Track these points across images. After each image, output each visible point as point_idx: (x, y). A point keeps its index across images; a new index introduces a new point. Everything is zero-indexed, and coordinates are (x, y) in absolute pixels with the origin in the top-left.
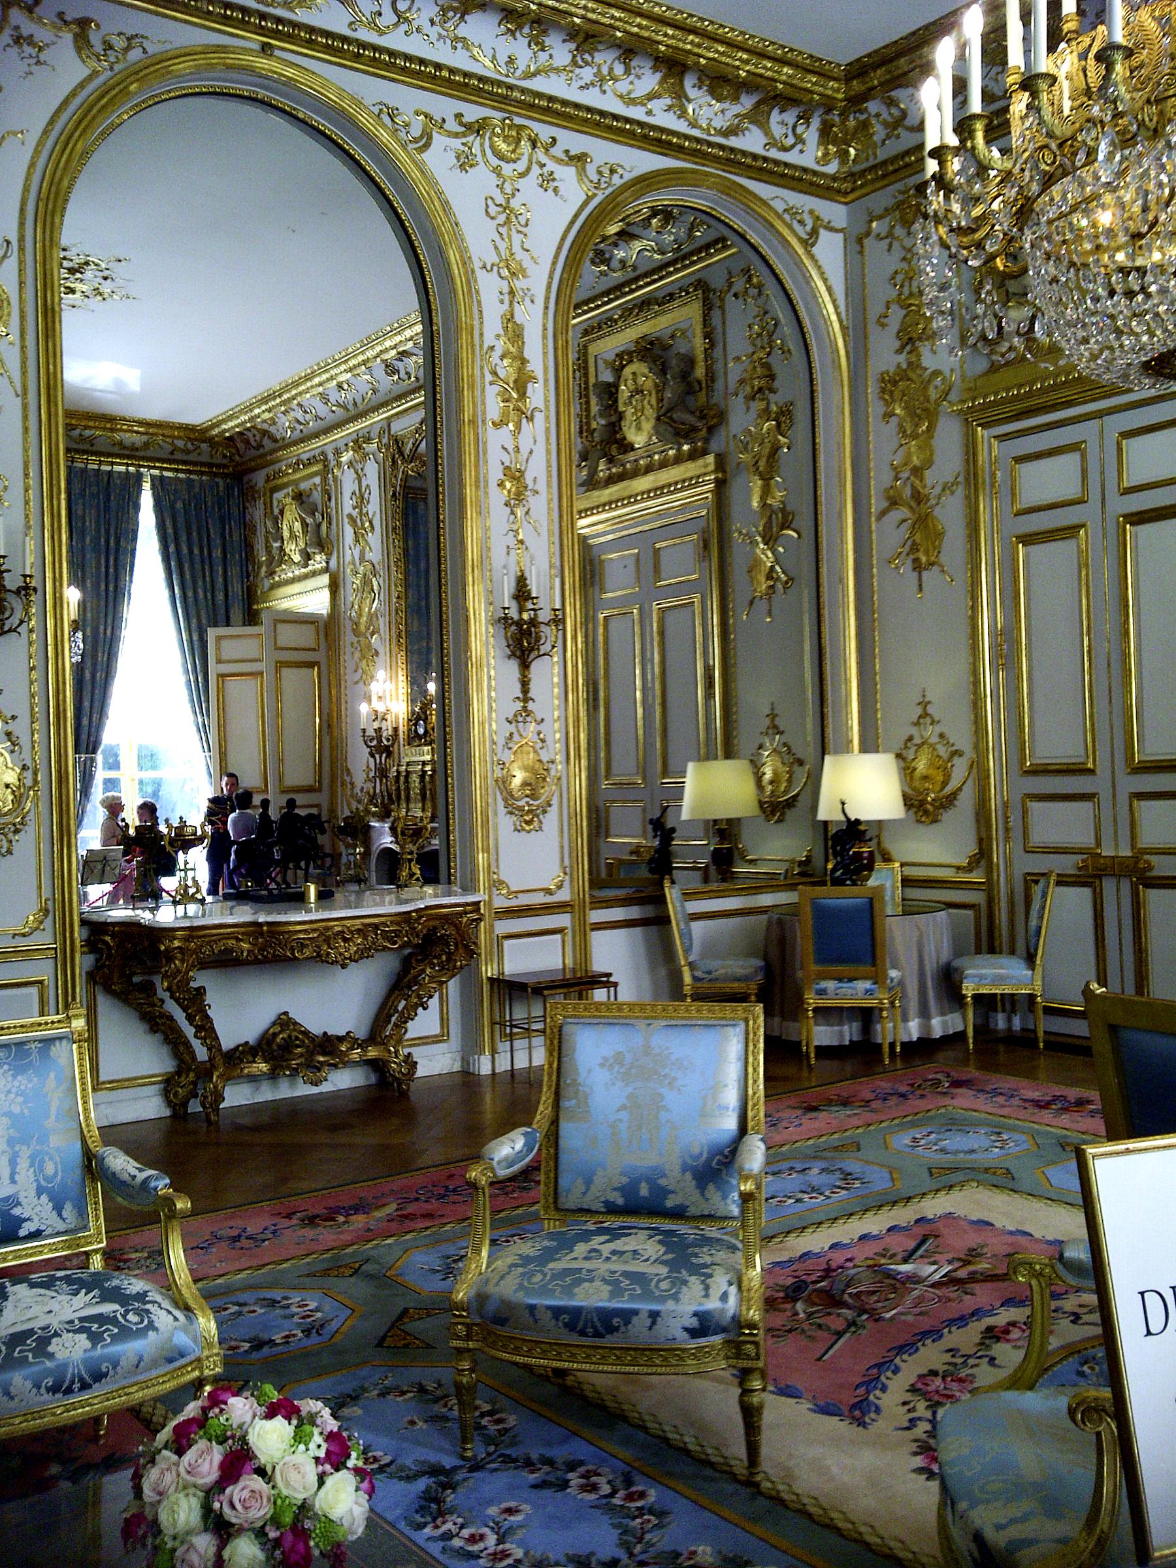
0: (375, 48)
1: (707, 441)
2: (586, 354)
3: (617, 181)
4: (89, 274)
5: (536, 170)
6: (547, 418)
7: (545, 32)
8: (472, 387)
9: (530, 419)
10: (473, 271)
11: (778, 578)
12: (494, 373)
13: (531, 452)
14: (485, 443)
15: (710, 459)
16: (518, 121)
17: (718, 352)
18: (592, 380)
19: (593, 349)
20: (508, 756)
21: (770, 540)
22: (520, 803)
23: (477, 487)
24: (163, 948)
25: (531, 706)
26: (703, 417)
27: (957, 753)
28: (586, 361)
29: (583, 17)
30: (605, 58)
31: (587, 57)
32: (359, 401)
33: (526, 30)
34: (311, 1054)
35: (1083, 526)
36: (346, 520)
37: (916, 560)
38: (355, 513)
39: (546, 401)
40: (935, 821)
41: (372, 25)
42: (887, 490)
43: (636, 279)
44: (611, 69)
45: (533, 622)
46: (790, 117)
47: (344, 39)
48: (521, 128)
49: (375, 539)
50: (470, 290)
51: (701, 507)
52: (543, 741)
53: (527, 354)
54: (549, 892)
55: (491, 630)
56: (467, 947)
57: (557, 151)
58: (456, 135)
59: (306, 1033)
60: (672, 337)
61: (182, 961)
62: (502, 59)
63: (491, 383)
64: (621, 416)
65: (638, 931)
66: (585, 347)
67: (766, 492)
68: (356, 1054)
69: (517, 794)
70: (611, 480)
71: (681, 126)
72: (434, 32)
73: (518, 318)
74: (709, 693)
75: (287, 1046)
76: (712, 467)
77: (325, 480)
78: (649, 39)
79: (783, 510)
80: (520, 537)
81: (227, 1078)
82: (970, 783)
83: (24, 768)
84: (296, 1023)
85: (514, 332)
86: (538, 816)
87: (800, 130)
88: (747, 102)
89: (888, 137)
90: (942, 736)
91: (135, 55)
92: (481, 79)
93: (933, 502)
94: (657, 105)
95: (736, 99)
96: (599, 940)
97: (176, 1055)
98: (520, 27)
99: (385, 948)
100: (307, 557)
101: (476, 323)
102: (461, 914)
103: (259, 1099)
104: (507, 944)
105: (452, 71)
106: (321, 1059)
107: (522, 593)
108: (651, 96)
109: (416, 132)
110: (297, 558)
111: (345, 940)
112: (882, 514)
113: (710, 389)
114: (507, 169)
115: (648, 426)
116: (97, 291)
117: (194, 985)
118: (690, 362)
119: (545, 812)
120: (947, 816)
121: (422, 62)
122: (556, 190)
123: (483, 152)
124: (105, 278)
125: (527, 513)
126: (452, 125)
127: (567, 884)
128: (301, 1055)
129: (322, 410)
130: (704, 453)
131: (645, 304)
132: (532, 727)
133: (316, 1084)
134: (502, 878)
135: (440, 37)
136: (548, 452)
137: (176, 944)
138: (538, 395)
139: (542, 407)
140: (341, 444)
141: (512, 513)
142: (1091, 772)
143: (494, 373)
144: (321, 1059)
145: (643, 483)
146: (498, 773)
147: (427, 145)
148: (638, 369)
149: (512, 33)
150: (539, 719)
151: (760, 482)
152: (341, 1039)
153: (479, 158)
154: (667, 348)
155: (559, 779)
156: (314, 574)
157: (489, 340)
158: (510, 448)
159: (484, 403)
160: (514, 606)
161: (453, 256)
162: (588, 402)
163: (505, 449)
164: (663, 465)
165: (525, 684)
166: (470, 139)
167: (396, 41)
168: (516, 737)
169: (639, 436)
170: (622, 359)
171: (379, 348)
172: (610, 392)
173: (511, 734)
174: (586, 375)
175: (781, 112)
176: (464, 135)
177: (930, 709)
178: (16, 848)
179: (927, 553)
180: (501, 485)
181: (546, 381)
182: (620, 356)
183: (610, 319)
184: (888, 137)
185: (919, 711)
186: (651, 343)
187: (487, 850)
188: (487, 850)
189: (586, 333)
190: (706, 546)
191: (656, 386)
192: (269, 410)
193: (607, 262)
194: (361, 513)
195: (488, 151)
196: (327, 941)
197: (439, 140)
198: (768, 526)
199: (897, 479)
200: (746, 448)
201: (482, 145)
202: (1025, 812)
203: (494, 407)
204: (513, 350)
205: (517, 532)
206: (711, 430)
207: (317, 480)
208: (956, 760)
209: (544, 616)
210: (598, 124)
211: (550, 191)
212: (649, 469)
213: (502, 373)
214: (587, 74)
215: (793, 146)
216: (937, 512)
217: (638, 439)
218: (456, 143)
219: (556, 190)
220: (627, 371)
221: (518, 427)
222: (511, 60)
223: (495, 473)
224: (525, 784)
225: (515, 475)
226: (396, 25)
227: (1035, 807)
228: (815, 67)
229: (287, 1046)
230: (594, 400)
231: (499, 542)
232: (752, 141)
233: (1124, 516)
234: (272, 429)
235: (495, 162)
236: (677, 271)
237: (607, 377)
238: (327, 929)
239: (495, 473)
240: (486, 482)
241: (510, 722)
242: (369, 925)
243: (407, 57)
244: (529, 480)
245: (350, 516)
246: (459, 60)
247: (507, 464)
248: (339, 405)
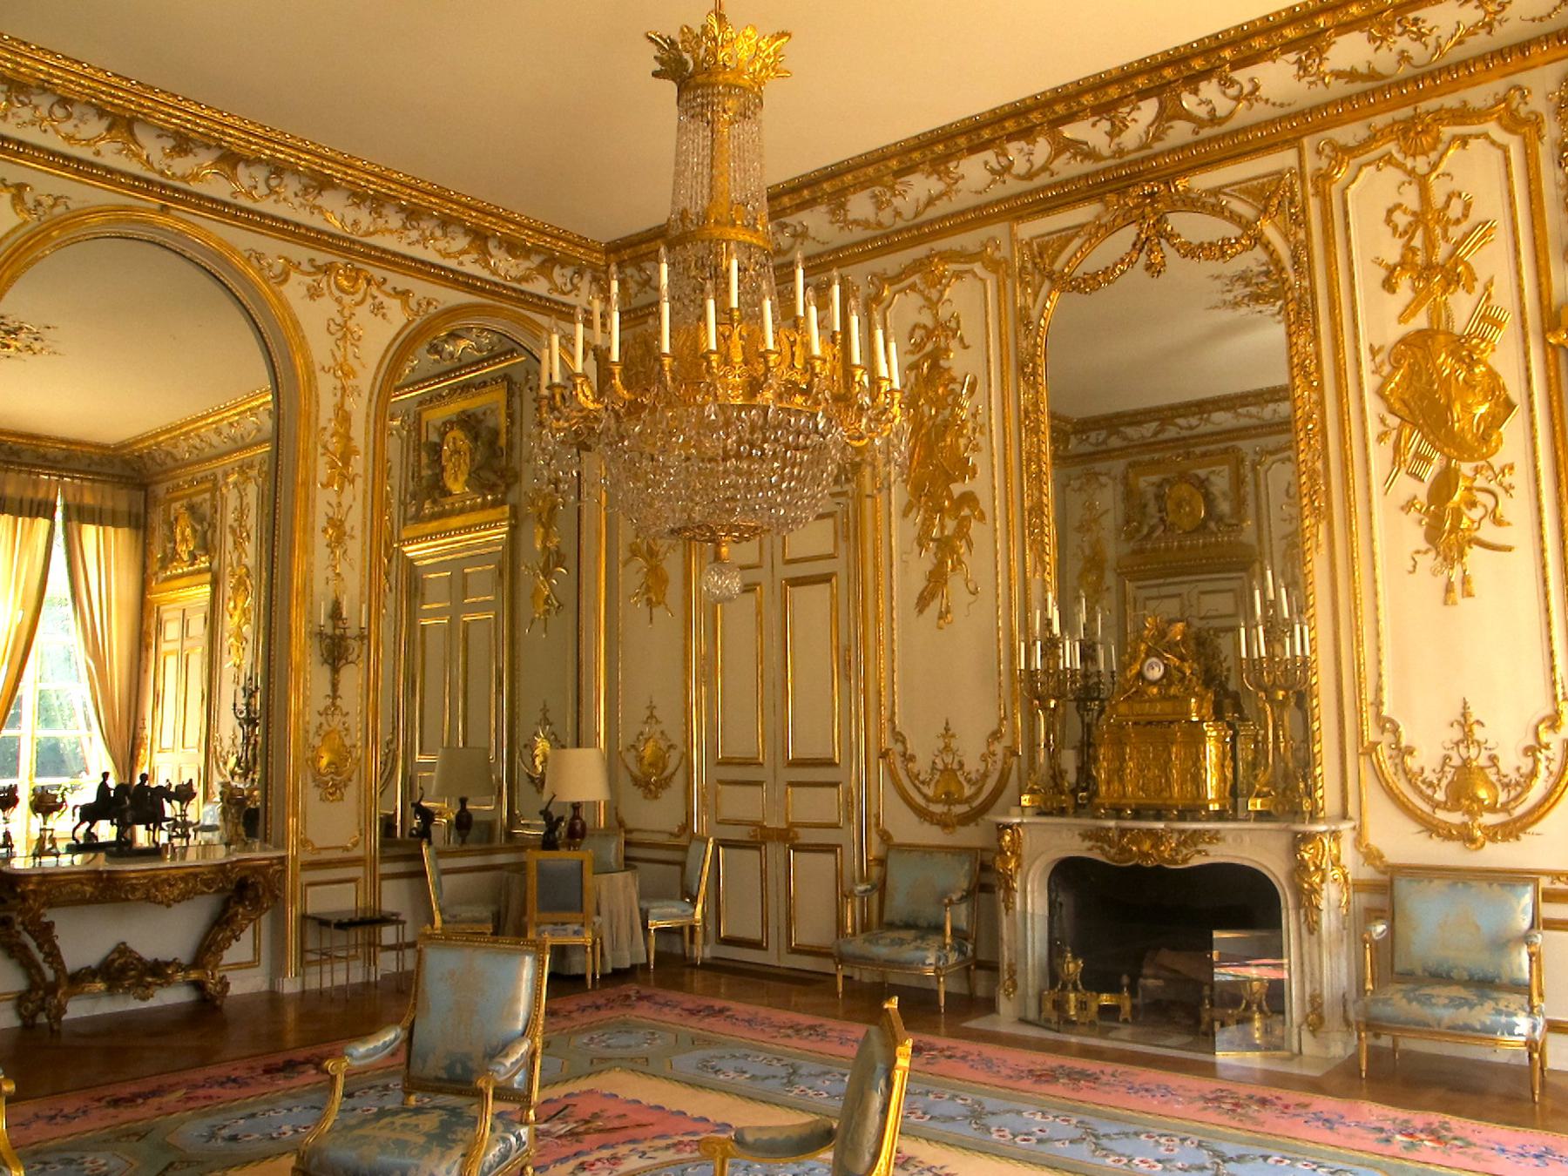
0: (249, 211)
1: (505, 494)
2: (420, 420)
3: (432, 310)
4: (22, 335)
5: (369, 300)
6: (365, 481)
7: (382, 206)
8: (306, 458)
9: (352, 482)
10: (314, 372)
11: (552, 605)
12: (325, 447)
14: (314, 500)
15: (507, 508)
16: (357, 265)
17: (516, 429)
18: (423, 439)
19: (426, 416)
20: (317, 741)
21: (547, 573)
22: (326, 779)
23: (305, 533)
24: (19, 890)
25: (338, 702)
26: (502, 477)
27: (671, 747)
28: (420, 425)
29: (407, 201)
30: (427, 225)
31: (415, 223)
32: (245, 435)
33: (368, 203)
34: (142, 975)
35: (759, 584)
36: (228, 530)
37: (649, 601)
38: (235, 525)
39: (366, 470)
40: (656, 797)
41: (249, 194)
42: (631, 545)
43: (460, 368)
44: (432, 234)
45: (343, 637)
46: (568, 272)
47: (226, 204)
48: (358, 270)
49: (250, 547)
50: (310, 385)
51: (497, 544)
52: (347, 729)
53: (352, 434)
54: (346, 849)
55: (309, 642)
56: (272, 892)
57: (387, 288)
58: (309, 274)
59: (140, 959)
60: (484, 414)
61: (35, 901)
62: (349, 221)
63: (323, 455)
64: (443, 469)
65: (404, 883)
66: (420, 414)
67: (546, 537)
68: (179, 976)
69: (322, 771)
70: (434, 517)
71: (485, 274)
72: (297, 201)
73: (347, 407)
74: (499, 691)
75: (123, 970)
76: (507, 515)
77: (213, 497)
78: (457, 218)
79: (558, 552)
81: (69, 995)
82: (681, 769)
84: (131, 951)
85: (344, 417)
87: (575, 281)
88: (536, 260)
89: (639, 291)
90: (662, 733)
91: (60, 209)
92: (331, 235)
93: (661, 557)
94: (466, 258)
95: (527, 257)
96: (388, 886)
97: (29, 976)
98: (363, 201)
99: (203, 893)
100: (194, 558)
101: (313, 410)
102: (268, 866)
103: (97, 1013)
104: (310, 890)
105: (308, 229)
106: (150, 979)
107: (336, 614)
108: (463, 252)
109: (277, 270)
110: (186, 557)
111: (170, 885)
112: (626, 563)
113: (509, 455)
114: (347, 299)
115: (463, 478)
116: (29, 347)
117: (45, 919)
118: (495, 433)
119: (345, 786)
120: (665, 795)
121: (285, 222)
122: (384, 316)
123: (329, 285)
124: (36, 339)
126: (306, 267)
127: (361, 844)
128: (132, 977)
129: (215, 440)
130: (503, 503)
131: (465, 387)
132: (337, 718)
133: (144, 999)
134: (308, 837)
135: (302, 205)
136: (364, 507)
137: (31, 887)
138: (358, 464)
139: (361, 472)
140: (229, 468)
142: (761, 764)
143: (325, 447)
144: (150, 979)
145: (456, 522)
146: (309, 754)
147: (285, 280)
148: (457, 433)
149: (358, 205)
150: (344, 711)
151: (542, 530)
152: (168, 964)
153: (326, 291)
154: (480, 422)
155: (359, 760)
156: (199, 572)
157: (322, 423)
159: (315, 470)
160: (330, 623)
161: (299, 361)
162: (419, 455)
163: (330, 504)
164: (473, 509)
165: (335, 686)
166: (319, 277)
167: (267, 206)
168: (325, 727)
169: (457, 486)
170: (449, 424)
171: (261, 401)
172: (436, 450)
173: (321, 724)
174: (419, 434)
175: (562, 268)
176: (314, 274)
177: (656, 713)
179: (656, 594)
180: (325, 531)
181: (366, 454)
182: (444, 424)
183: (440, 395)
184: (639, 291)
185: (648, 713)
186: (469, 416)
187: (295, 814)
188: (295, 814)
189: (421, 403)
190: (501, 574)
191: (470, 449)
192: (172, 438)
193: (439, 353)
194: (240, 526)
195: (333, 287)
196: (155, 886)
197: (294, 276)
198: (547, 563)
199: (637, 537)
200: (533, 504)
201: (328, 282)
202: (717, 794)
203: (323, 471)
204: (342, 431)
205: (335, 567)
206: (508, 487)
207: (207, 496)
208: (672, 752)
209: (353, 631)
210: (420, 271)
211: (380, 316)
212: (462, 511)
213: (331, 447)
214: (414, 235)
215: (571, 291)
216: (664, 565)
217: (457, 488)
218: (309, 280)
219: (384, 316)
220: (449, 437)
221: (341, 488)
222: (355, 223)
223: (321, 521)
224: (329, 765)
225: (336, 524)
226: (267, 196)
227: (726, 790)
228: (581, 242)
229: (123, 970)
230: (423, 454)
231: (320, 574)
232: (540, 287)
233: (786, 580)
234: (174, 451)
235: (337, 293)
236: (489, 366)
237: (434, 438)
238: (155, 876)
239: (321, 521)
240: (313, 529)
241: (321, 714)
242: (191, 874)
243: (274, 218)
244: (347, 527)
245: (231, 526)
246: (316, 221)
247: (331, 514)
248: (230, 438)
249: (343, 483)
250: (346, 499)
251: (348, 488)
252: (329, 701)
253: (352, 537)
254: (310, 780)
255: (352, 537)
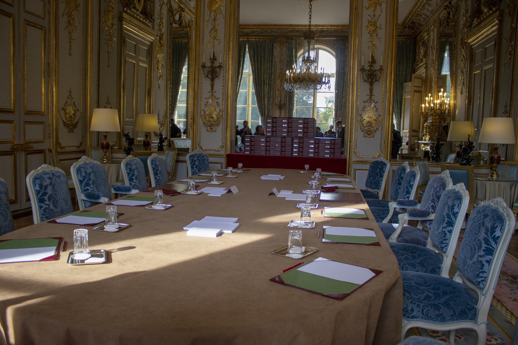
6: (387, 4)
13: (380, 16)
25: (373, 97)
69: (365, 125)
80: (373, 43)
83: (220, 111)
86: (373, 133)
119: (376, 132)
125: (377, 35)
141: (371, 35)
150: (376, 102)
158: (372, 15)
165: (371, 91)
178: (217, 130)
223: (365, 23)
225: (373, 24)
239: (365, 23)
244: (378, 24)
247: (370, 20)
249: (376, 7)
250: (377, 13)
251: (378, 7)
252: (368, 97)
253: (381, 28)
254: (359, 128)
255: (381, 28)
